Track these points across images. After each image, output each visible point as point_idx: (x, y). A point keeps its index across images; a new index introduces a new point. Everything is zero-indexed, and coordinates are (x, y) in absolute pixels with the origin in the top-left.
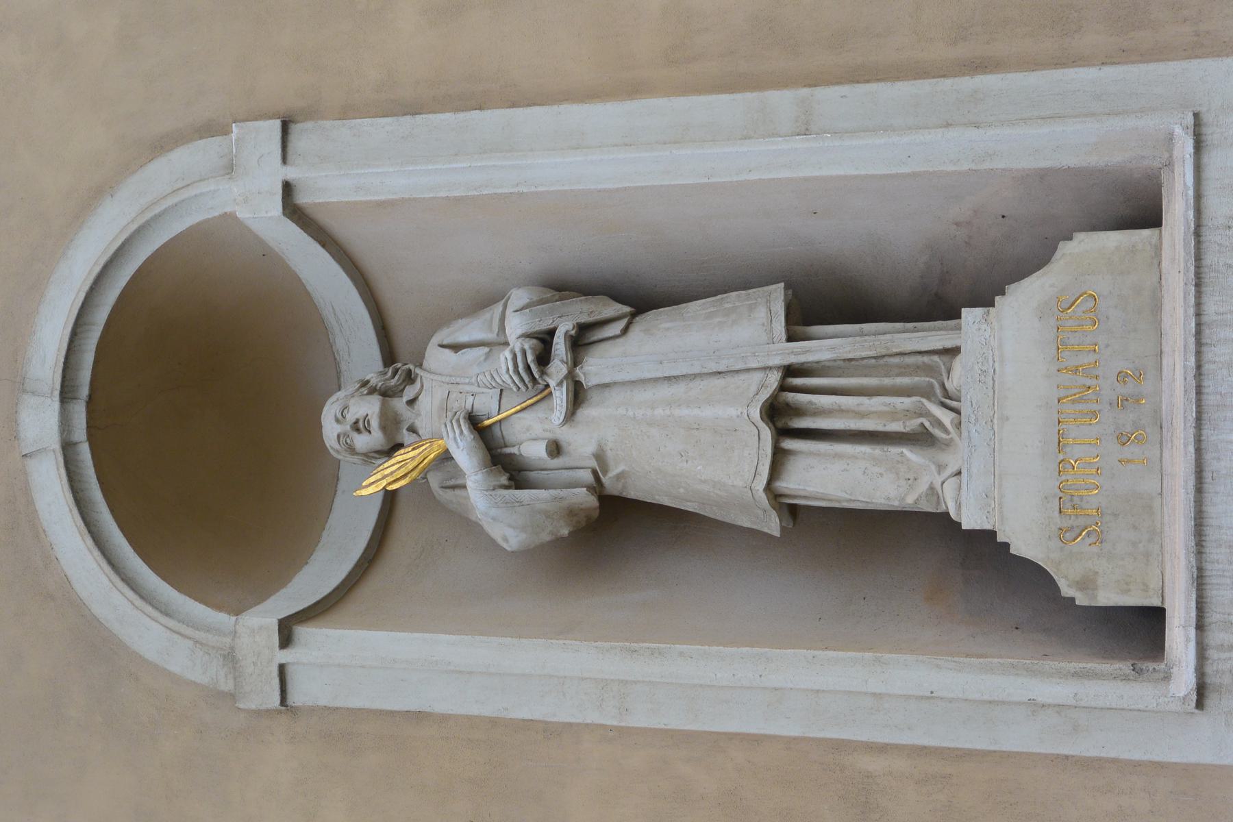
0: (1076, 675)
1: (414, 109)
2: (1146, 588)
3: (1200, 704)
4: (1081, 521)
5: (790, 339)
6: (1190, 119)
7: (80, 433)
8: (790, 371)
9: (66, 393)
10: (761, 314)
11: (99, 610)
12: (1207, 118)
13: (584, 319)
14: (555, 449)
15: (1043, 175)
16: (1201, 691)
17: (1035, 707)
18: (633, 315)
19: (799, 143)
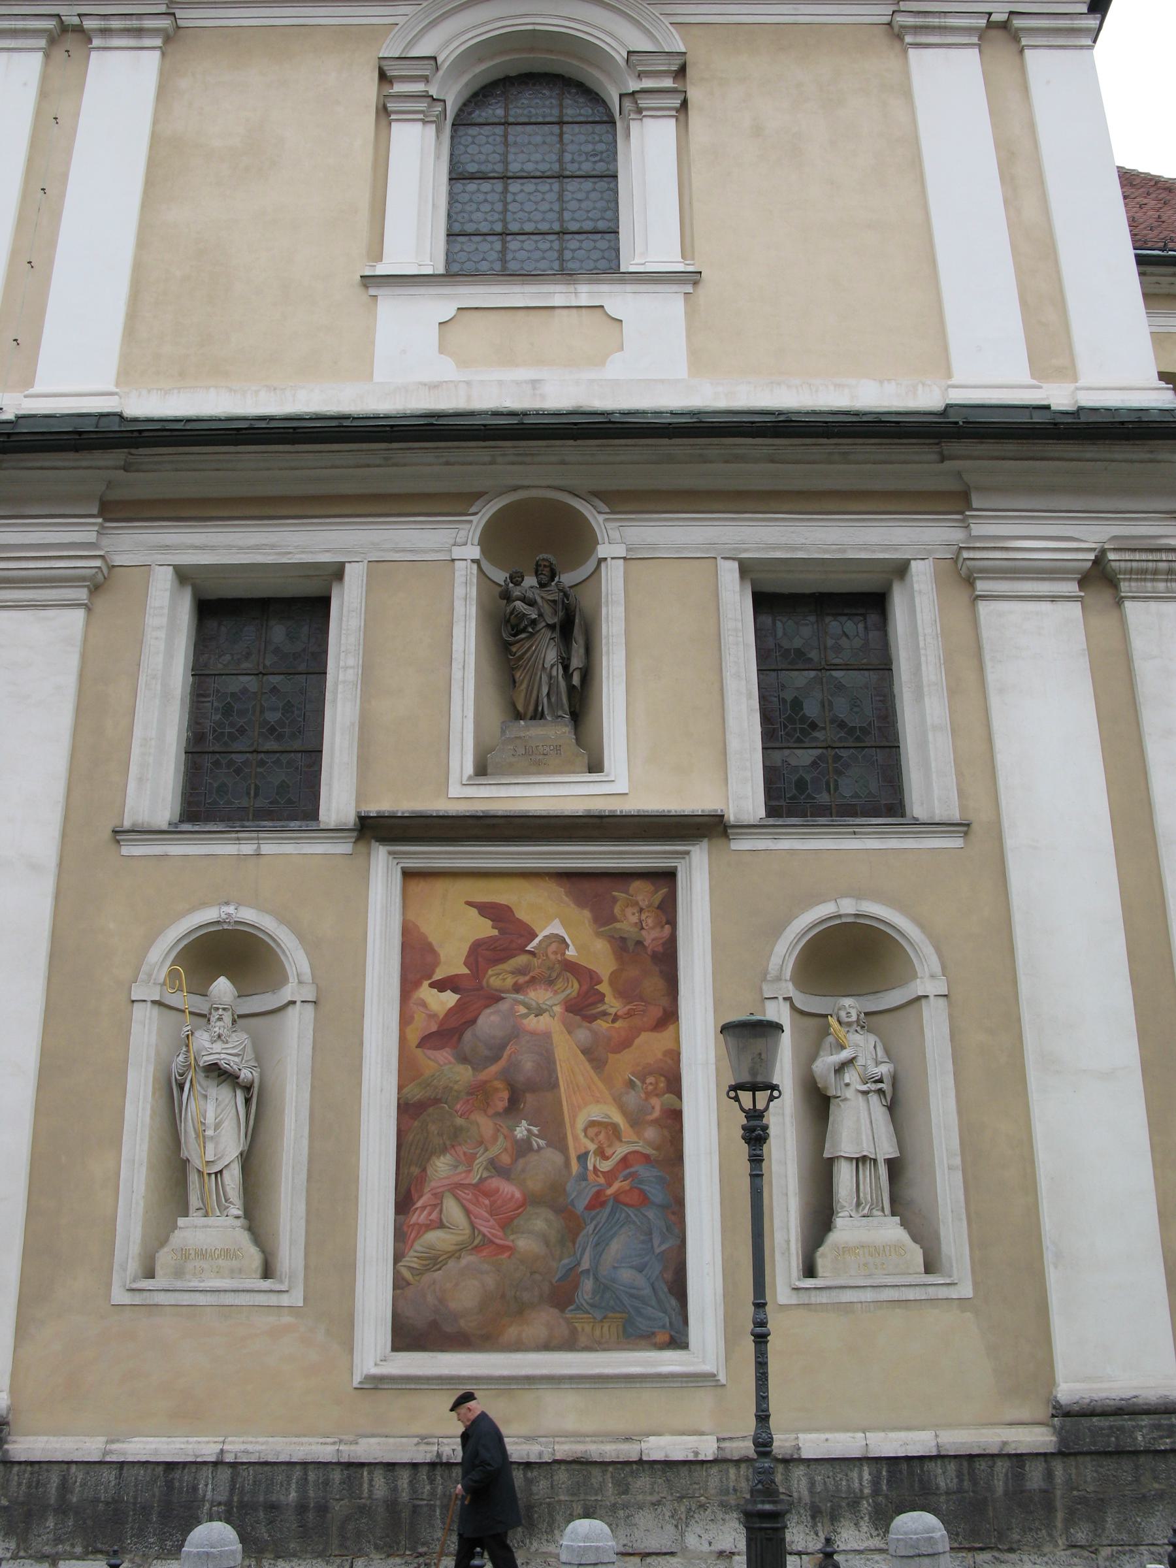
0: (797, 1253)
1: (952, 1040)
2: (824, 1272)
3: (794, 1289)
4: (841, 1253)
5: (885, 1160)
6: (956, 1282)
7: (844, 920)
8: (875, 1160)
9: (857, 916)
10: (891, 1150)
11: (788, 929)
12: (956, 1287)
13: (887, 1092)
14: (847, 1085)
15: (938, 1239)
16: (797, 1289)
17: (788, 1242)
18: (887, 1106)
19: (946, 1166)
